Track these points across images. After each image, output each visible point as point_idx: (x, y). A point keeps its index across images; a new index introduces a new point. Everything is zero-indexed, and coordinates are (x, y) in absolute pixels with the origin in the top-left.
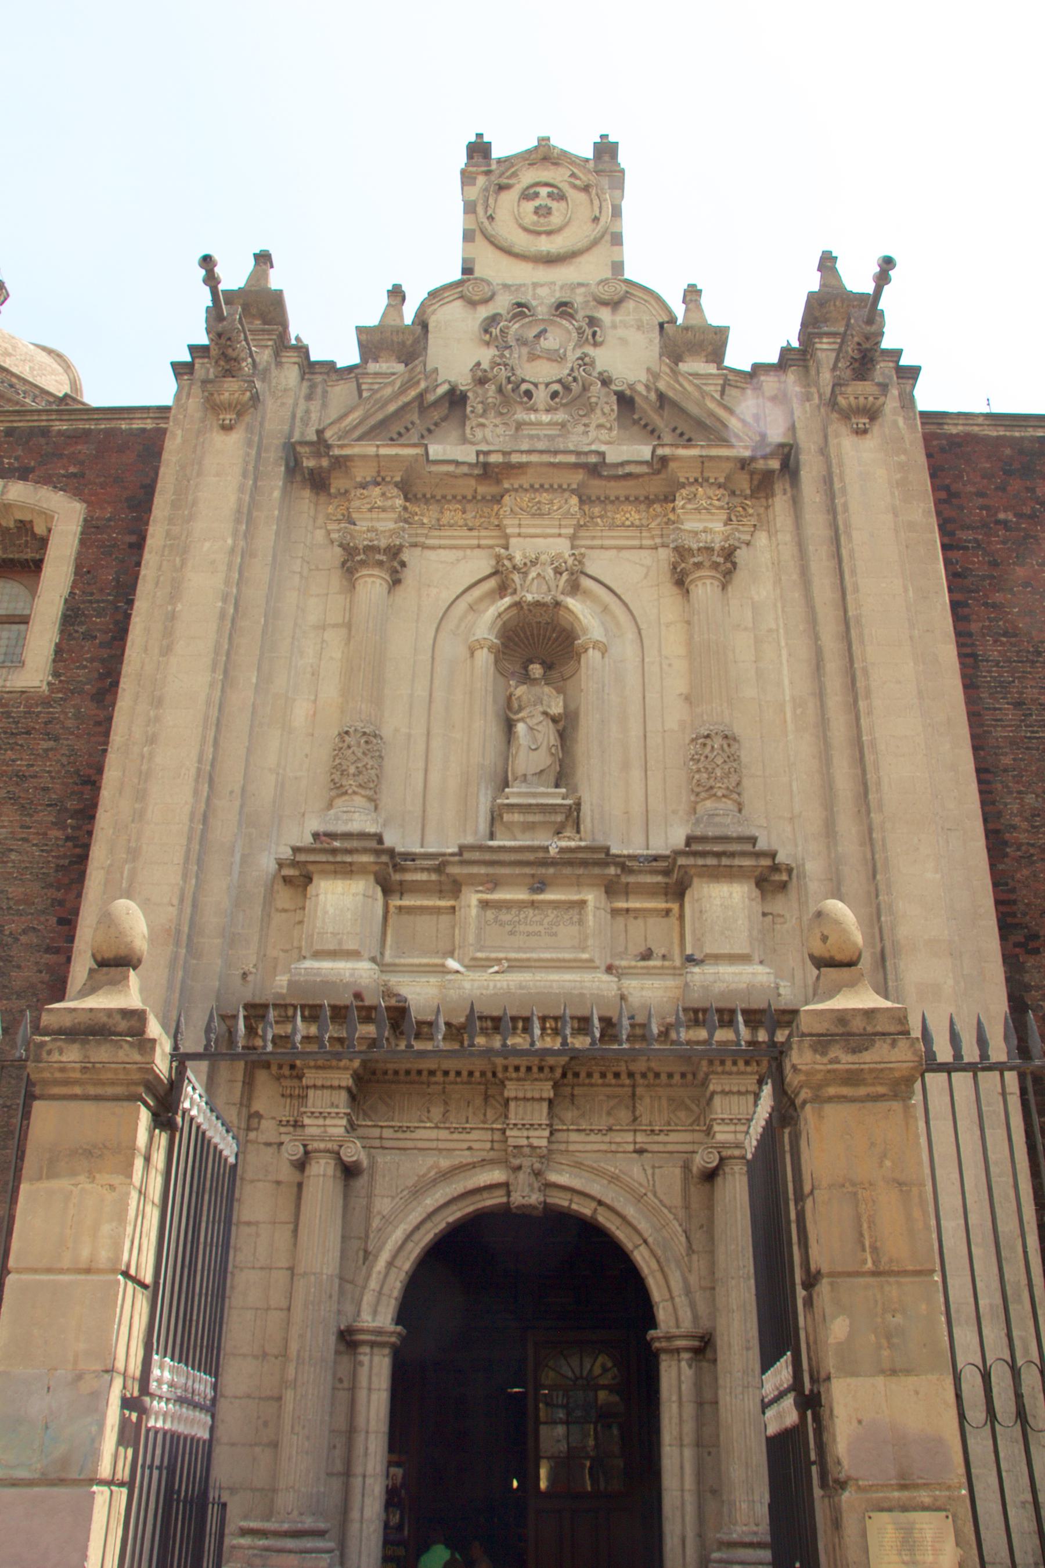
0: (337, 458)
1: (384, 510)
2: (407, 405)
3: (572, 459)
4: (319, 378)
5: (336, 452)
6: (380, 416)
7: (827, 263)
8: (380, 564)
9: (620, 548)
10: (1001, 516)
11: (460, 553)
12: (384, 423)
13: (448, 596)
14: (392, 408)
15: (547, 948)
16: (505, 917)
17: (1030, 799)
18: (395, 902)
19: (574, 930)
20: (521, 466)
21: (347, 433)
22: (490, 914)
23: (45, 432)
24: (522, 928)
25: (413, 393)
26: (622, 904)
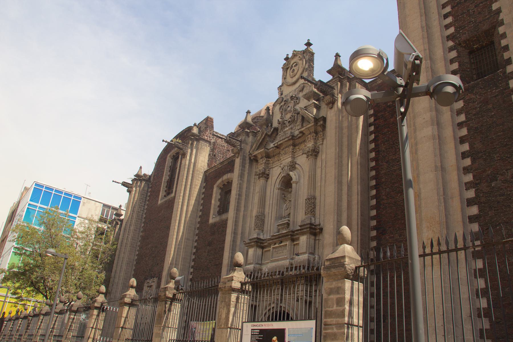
0: (254, 156)
3: (287, 139)
7: (337, 56)
12: (261, 143)
15: (282, 256)
17: (387, 190)
20: (281, 144)
26: (295, 243)
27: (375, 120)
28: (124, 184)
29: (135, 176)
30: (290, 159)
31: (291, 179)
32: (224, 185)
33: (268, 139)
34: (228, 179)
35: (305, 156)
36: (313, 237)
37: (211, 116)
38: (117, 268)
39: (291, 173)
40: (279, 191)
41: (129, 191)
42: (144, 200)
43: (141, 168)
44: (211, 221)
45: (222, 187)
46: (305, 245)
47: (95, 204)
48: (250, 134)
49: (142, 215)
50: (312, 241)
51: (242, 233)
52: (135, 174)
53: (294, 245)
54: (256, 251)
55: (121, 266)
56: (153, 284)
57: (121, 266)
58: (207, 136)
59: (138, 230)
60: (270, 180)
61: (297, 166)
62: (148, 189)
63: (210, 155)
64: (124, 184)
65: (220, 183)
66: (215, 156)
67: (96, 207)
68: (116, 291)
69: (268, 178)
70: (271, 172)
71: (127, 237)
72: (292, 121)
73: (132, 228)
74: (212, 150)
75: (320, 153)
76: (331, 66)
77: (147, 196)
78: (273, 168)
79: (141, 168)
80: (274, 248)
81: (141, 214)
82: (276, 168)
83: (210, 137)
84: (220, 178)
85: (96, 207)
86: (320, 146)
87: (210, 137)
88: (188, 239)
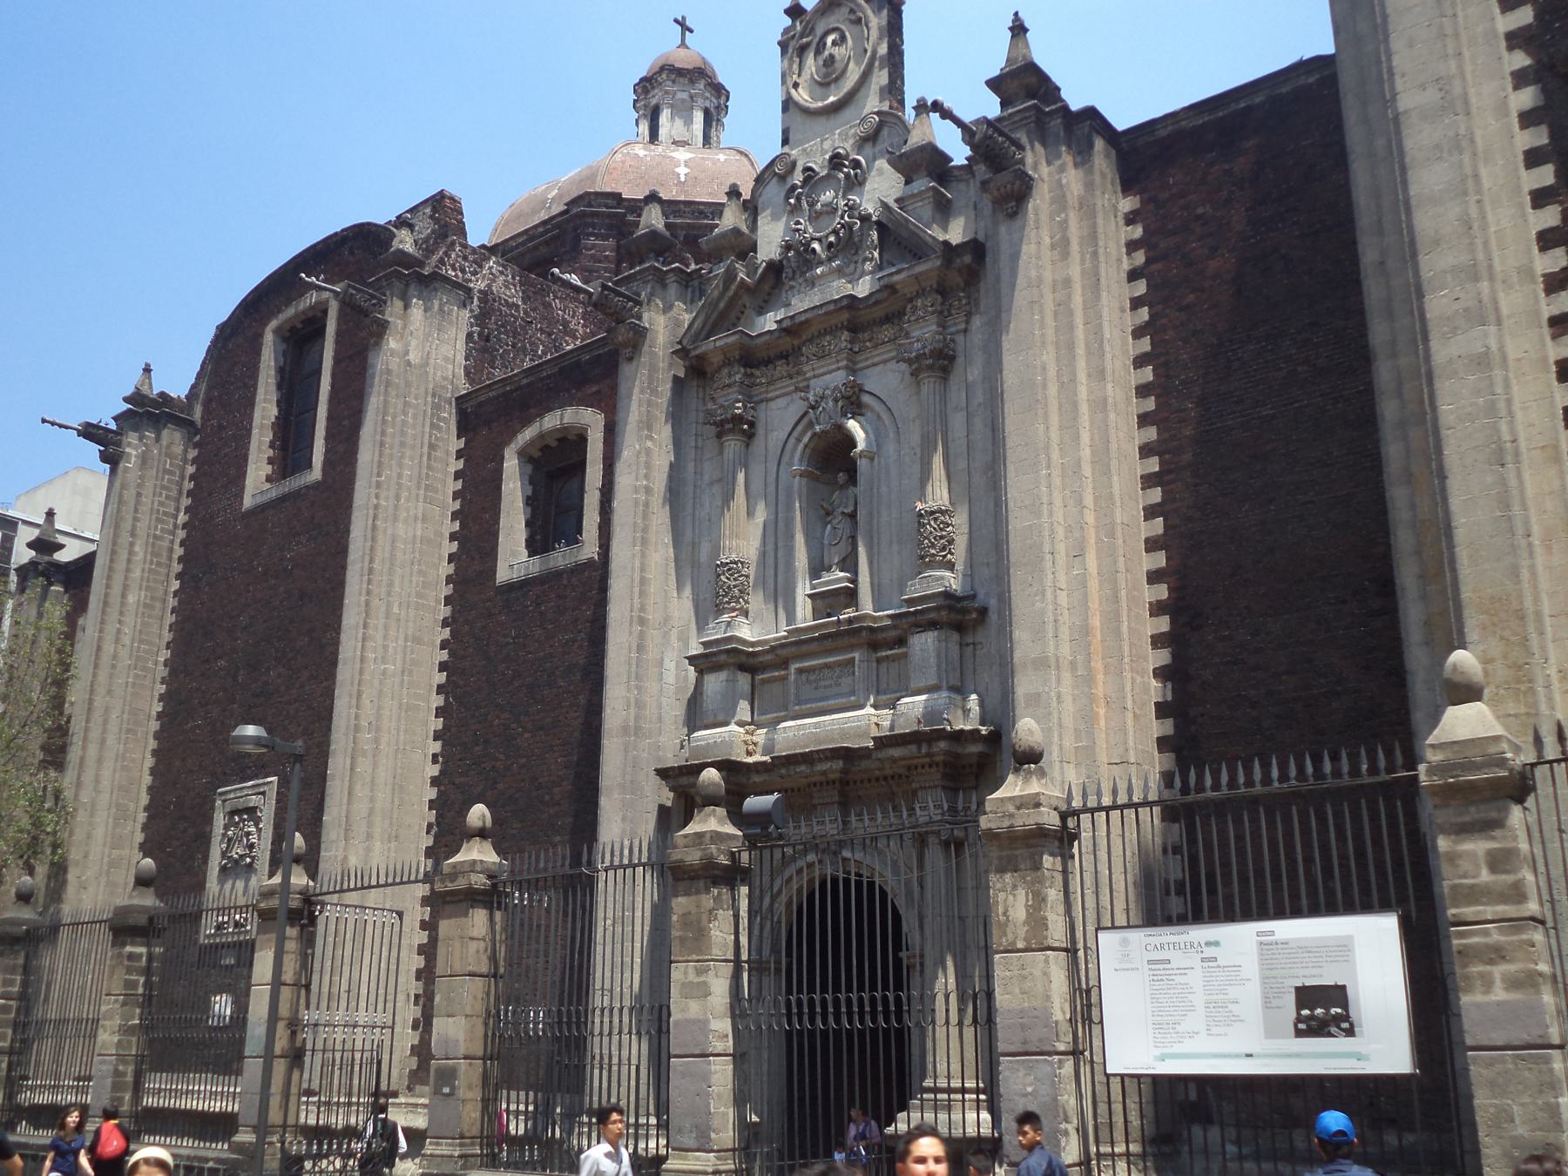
0: (697, 357)
1: (729, 386)
2: (736, 294)
4: (696, 283)
5: (693, 353)
6: (715, 315)
8: (731, 431)
9: (885, 362)
10: (1200, 211)
11: (787, 399)
13: (784, 435)
14: (722, 305)
16: (812, 678)
18: (759, 677)
19: (850, 679)
21: (698, 334)
22: (804, 677)
23: (578, 364)
24: (822, 683)
25: (733, 287)
27: (1149, 261)
28: (90, 432)
30: (839, 378)
31: (852, 443)
32: (545, 449)
33: (746, 300)
34: (565, 429)
35: (903, 366)
36: (955, 637)
37: (452, 190)
38: (84, 748)
39: (853, 425)
40: (804, 480)
41: (112, 458)
42: (174, 494)
43: (147, 370)
44: (503, 575)
45: (536, 454)
46: (933, 660)
48: (671, 278)
49: (171, 550)
50: (955, 650)
52: (129, 391)
53: (879, 661)
54: (734, 681)
55: (103, 741)
56: (254, 800)
58: (454, 269)
60: (759, 442)
61: (866, 398)
62: (186, 451)
63: (469, 336)
64: (90, 432)
65: (532, 442)
66: (488, 340)
70: (762, 415)
71: (119, 631)
72: (846, 246)
73: (131, 599)
74: (481, 318)
75: (960, 360)
76: (996, 64)
78: (768, 400)
79: (147, 370)
80: (800, 671)
81: (166, 544)
82: (781, 402)
83: (463, 271)
84: (526, 422)
86: (960, 339)
87: (463, 271)
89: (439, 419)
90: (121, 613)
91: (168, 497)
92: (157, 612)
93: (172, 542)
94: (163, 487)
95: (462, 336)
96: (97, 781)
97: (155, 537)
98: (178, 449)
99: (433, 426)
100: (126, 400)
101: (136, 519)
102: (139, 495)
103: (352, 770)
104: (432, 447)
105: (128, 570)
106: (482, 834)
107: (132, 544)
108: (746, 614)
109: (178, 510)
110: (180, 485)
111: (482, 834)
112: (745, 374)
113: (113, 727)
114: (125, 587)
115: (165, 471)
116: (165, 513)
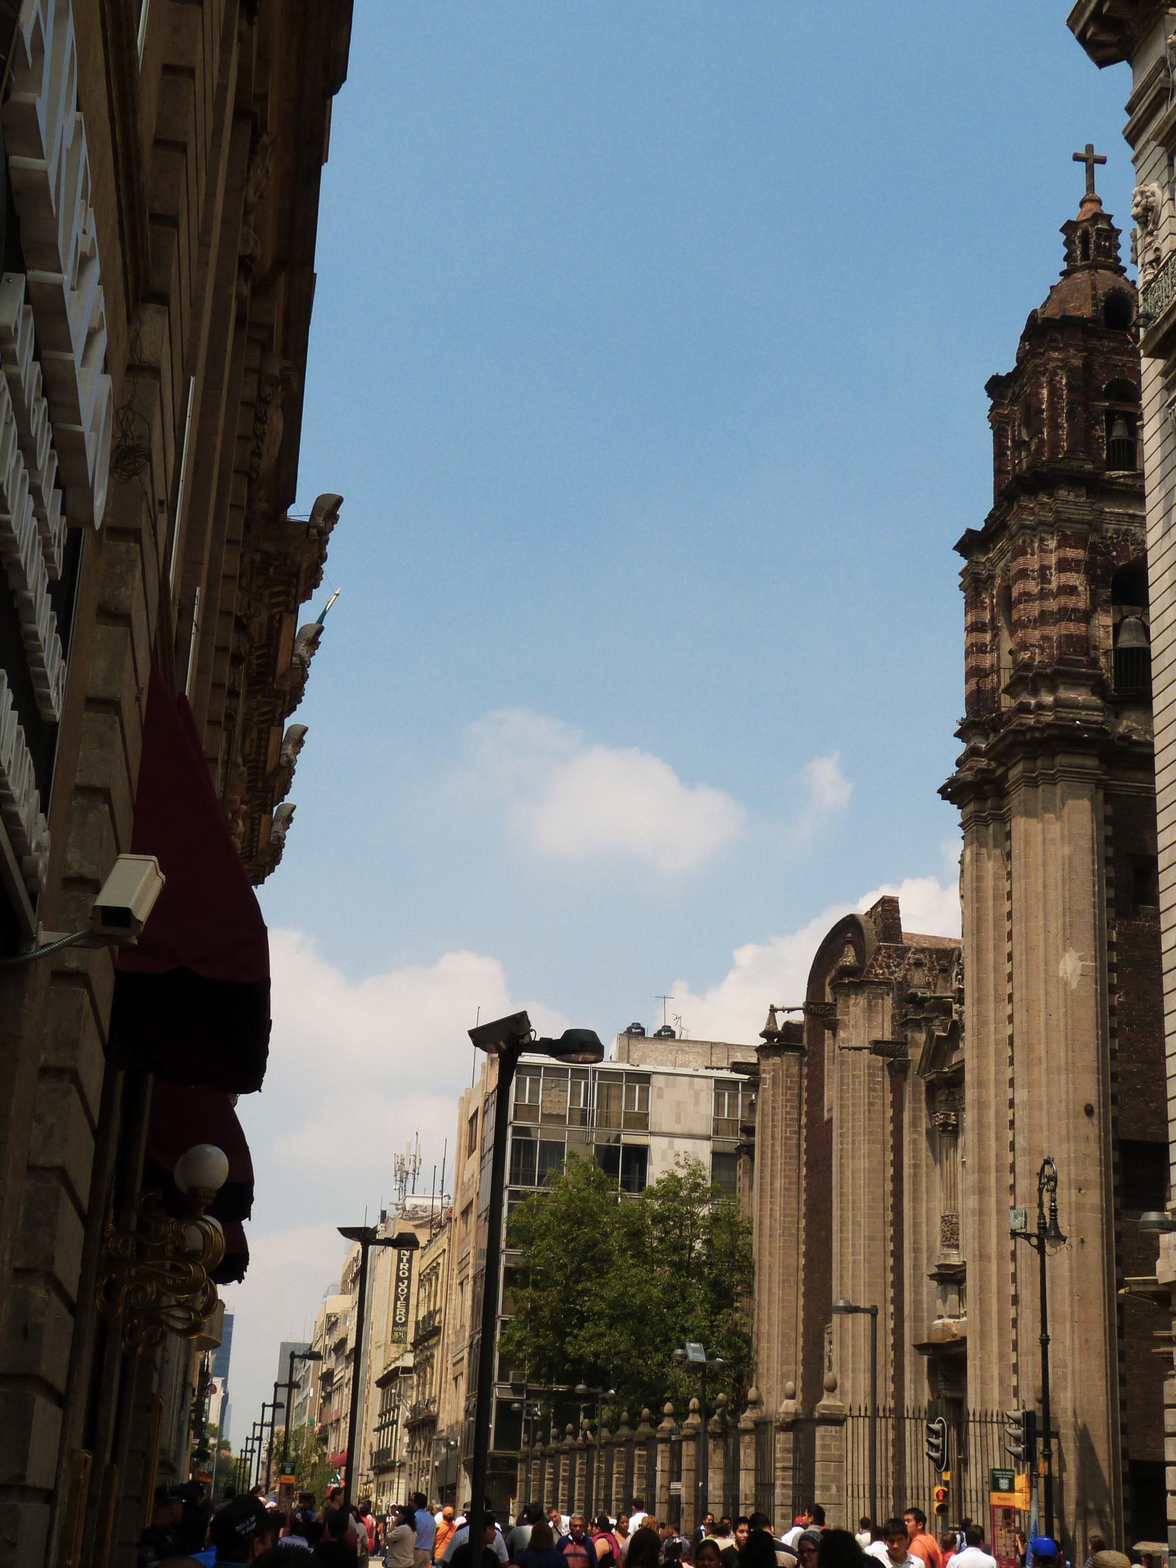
29: (762, 1035)
42: (796, 1103)
47: (691, 1084)
49: (799, 1145)
51: (928, 1248)
55: (770, 1289)
57: (770, 1289)
58: (881, 968)
59: (794, 1187)
62: (801, 1069)
63: (893, 1017)
67: (697, 1094)
68: (768, 1357)
69: (957, 1132)
71: (771, 1210)
73: (777, 1185)
77: (800, 1088)
81: (795, 1141)
83: (888, 967)
85: (697, 1094)
87: (888, 967)
88: (871, 1238)
89: (875, 1083)
90: (771, 1197)
91: (792, 1107)
92: (794, 1193)
93: (799, 1139)
94: (787, 1101)
95: (888, 1018)
96: (769, 1317)
97: (786, 1138)
98: (795, 1070)
99: (870, 1090)
100: (762, 1035)
101: (774, 1126)
102: (773, 1108)
103: (841, 1326)
104: (871, 1104)
105: (772, 1165)
106: (694, 1411)
107: (773, 1145)
108: (957, 1247)
109: (800, 1114)
110: (800, 1096)
111: (694, 1411)
112: (950, 1093)
113: (776, 1279)
114: (772, 1177)
115: (788, 1088)
116: (791, 1120)
